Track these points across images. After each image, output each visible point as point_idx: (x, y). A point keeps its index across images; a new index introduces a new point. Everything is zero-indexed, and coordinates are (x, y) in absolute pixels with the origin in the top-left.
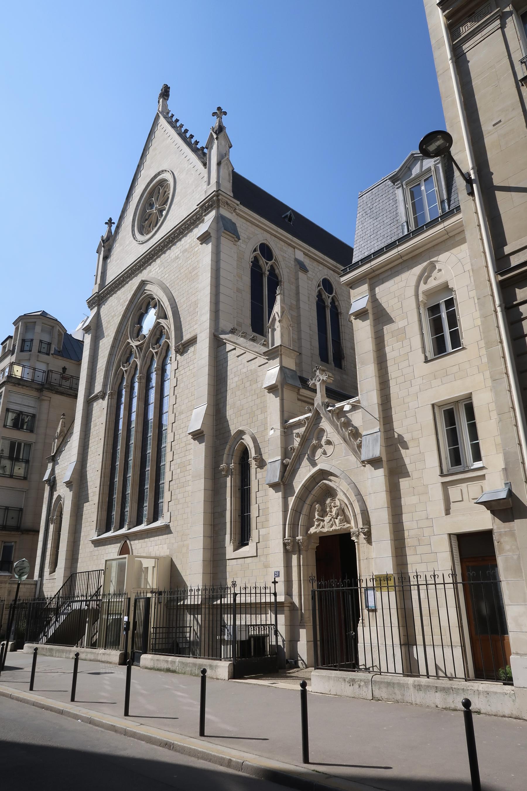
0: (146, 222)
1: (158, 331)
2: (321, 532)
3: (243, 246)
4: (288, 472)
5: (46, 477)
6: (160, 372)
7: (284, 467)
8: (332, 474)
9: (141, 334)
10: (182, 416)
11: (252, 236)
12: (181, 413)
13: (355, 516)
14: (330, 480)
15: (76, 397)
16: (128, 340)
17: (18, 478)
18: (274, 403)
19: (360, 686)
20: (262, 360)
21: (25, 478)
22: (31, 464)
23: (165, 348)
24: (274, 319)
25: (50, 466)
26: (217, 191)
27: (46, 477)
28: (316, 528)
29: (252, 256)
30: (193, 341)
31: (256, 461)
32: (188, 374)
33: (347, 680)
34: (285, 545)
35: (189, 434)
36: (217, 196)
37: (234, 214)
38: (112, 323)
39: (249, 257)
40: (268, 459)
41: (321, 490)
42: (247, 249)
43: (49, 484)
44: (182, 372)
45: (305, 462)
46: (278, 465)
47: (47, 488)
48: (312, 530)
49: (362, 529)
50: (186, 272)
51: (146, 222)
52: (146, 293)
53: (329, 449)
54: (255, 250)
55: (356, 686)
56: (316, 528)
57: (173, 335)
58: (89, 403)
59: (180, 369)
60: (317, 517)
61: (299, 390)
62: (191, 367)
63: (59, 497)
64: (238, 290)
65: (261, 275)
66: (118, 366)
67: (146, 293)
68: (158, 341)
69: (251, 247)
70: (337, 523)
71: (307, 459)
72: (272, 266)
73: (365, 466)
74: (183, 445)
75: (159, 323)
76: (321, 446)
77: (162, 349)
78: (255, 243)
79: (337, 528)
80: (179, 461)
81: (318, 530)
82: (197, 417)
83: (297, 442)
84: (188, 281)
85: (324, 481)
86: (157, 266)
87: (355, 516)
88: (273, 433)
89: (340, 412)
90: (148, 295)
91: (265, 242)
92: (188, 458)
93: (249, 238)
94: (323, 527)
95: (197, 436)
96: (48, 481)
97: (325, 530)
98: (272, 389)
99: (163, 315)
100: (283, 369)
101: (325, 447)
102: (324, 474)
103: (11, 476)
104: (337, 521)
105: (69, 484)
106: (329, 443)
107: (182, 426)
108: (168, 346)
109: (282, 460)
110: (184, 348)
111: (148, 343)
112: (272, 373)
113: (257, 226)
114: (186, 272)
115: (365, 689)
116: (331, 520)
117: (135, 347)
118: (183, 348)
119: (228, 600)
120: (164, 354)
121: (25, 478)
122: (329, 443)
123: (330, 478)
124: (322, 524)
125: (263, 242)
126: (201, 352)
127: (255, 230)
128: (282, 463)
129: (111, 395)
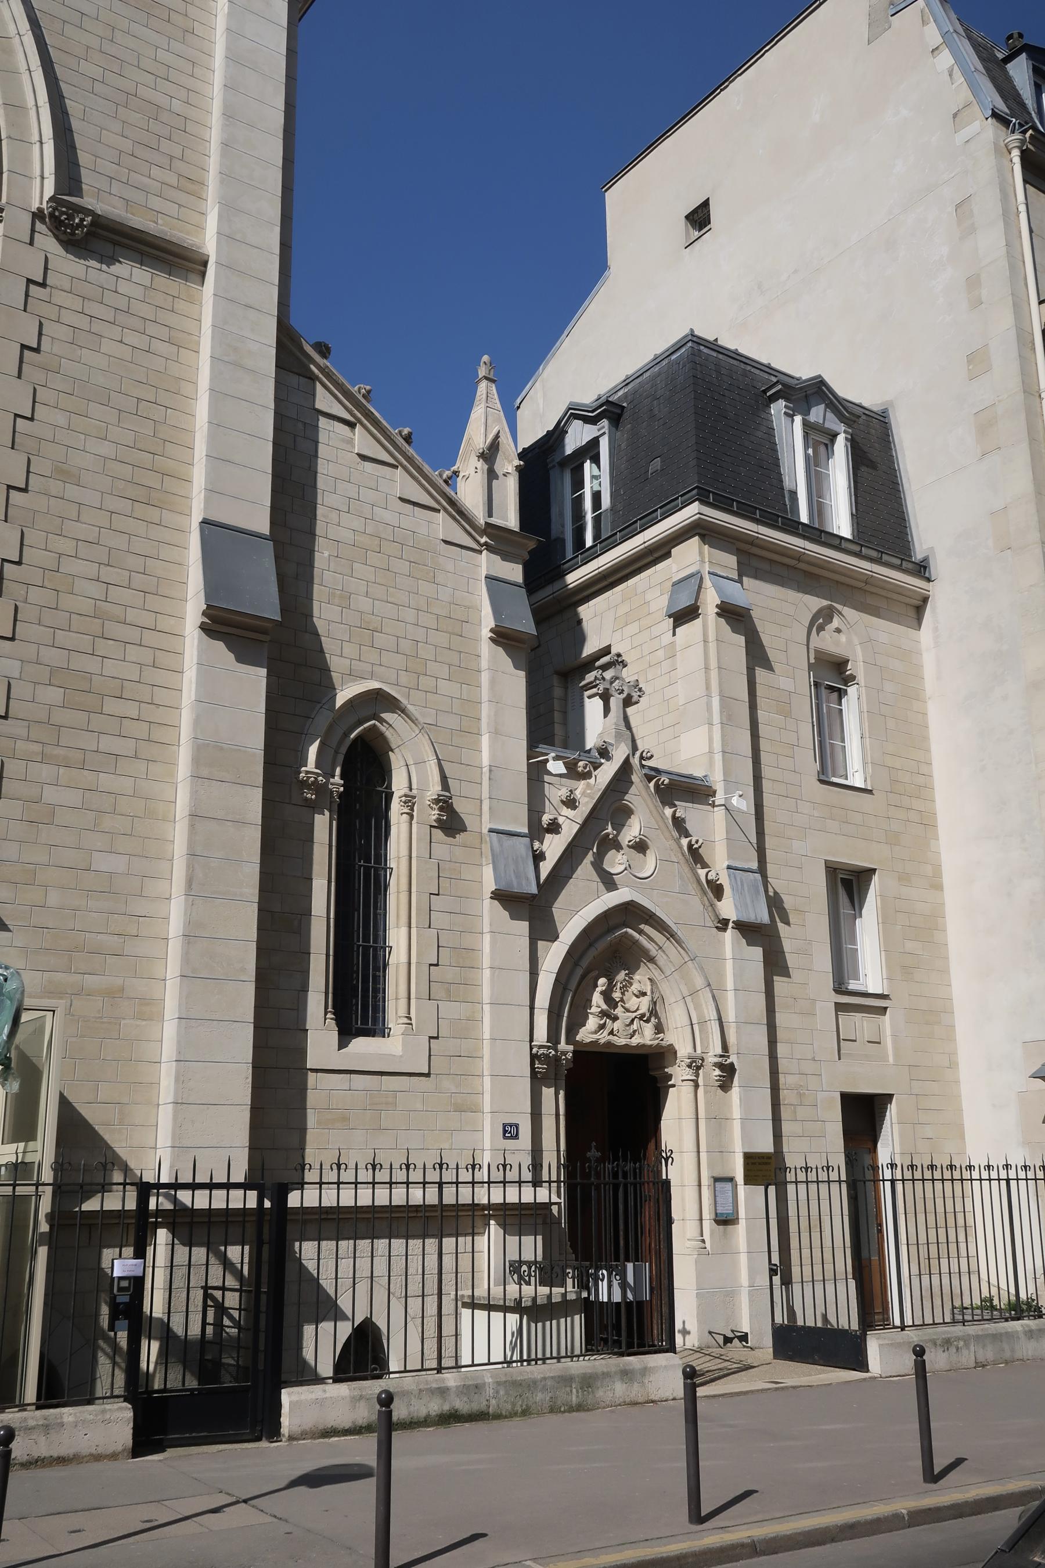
2: (609, 1044)
14: (641, 932)
19: (957, 1349)
31: (441, 809)
33: (939, 1342)
34: (533, 1058)
45: (585, 869)
49: (721, 1056)
55: (953, 1350)
71: (592, 863)
76: (618, 847)
81: (603, 1037)
85: (629, 931)
94: (611, 1033)
97: (620, 1041)
102: (630, 914)
115: (965, 1352)
116: (633, 1021)
119: (118, 1201)
123: (642, 926)
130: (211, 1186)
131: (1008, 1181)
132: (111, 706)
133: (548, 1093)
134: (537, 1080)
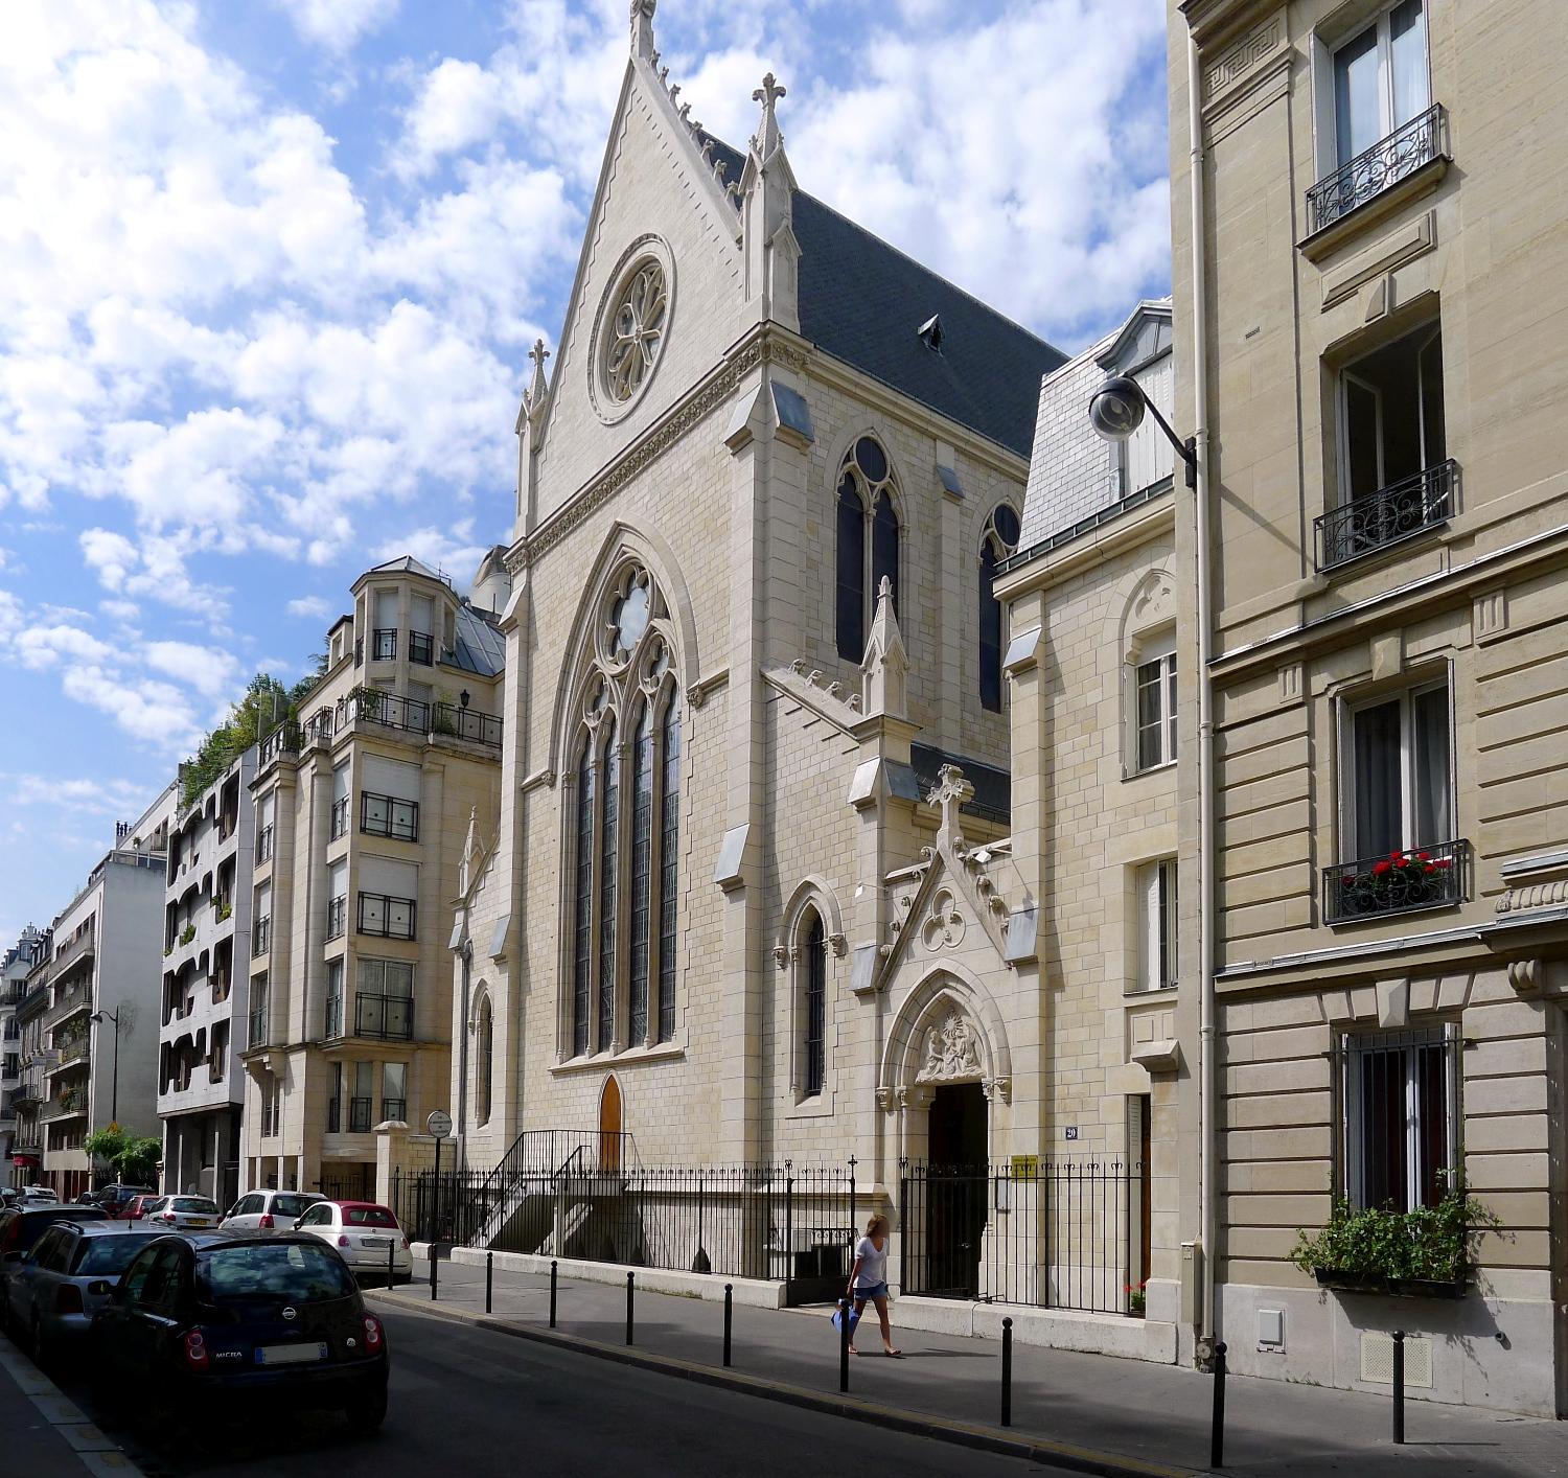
0: (623, 367)
1: (654, 647)
3: (822, 452)
4: (887, 967)
5: (454, 942)
6: (660, 740)
7: (881, 958)
8: (959, 980)
9: (619, 648)
10: (707, 841)
11: (840, 424)
12: (702, 835)
13: (990, 1055)
15: (496, 762)
16: (594, 661)
17: (397, 938)
18: (867, 834)
20: (848, 742)
21: (412, 938)
22: (419, 908)
23: (668, 687)
24: (873, 654)
25: (459, 917)
26: (764, 323)
27: (454, 942)
28: (928, 1073)
29: (840, 474)
30: (721, 681)
32: (713, 752)
35: (718, 883)
36: (764, 334)
37: (802, 375)
38: (561, 615)
39: (833, 478)
40: (854, 945)
41: (938, 1003)
42: (830, 458)
43: (462, 955)
44: (703, 748)
46: (871, 955)
47: (458, 963)
48: (923, 1076)
50: (706, 514)
51: (623, 367)
52: (625, 553)
53: (957, 931)
54: (848, 458)
56: (928, 1073)
57: (681, 660)
58: (525, 793)
59: (700, 740)
60: (931, 1053)
61: (915, 806)
62: (719, 739)
63: (482, 983)
64: (812, 565)
65: (860, 517)
66: (578, 716)
67: (625, 553)
68: (653, 668)
69: (838, 453)
70: (962, 1067)
72: (884, 491)
73: (1010, 969)
74: (708, 899)
75: (653, 629)
77: (662, 688)
78: (847, 441)
79: (962, 1075)
80: (700, 931)
82: (731, 854)
83: (901, 914)
84: (709, 539)
85: (945, 990)
86: (646, 490)
87: (990, 1055)
88: (865, 893)
89: (973, 865)
90: (629, 558)
91: (868, 434)
92: (717, 927)
93: (834, 430)
95: (732, 887)
96: (458, 949)
97: (943, 1077)
98: (864, 806)
99: (661, 611)
100: (886, 762)
101: (949, 926)
102: (941, 977)
103: (385, 934)
104: (963, 1063)
105: (499, 960)
106: (956, 919)
107: (706, 861)
108: (675, 684)
109: (879, 946)
110: (705, 694)
111: (635, 673)
112: (864, 776)
113: (853, 396)
114: (706, 514)
117: (609, 679)
118: (701, 696)
120: (665, 698)
121: (412, 938)
122: (956, 919)
124: (938, 1068)
125: (865, 434)
126: (739, 698)
127: (849, 405)
128: (879, 954)
129: (568, 779)
130: (536, 1180)
131: (701, 1181)
132: (718, 946)
133: (891, 1121)
134: (880, 1112)
